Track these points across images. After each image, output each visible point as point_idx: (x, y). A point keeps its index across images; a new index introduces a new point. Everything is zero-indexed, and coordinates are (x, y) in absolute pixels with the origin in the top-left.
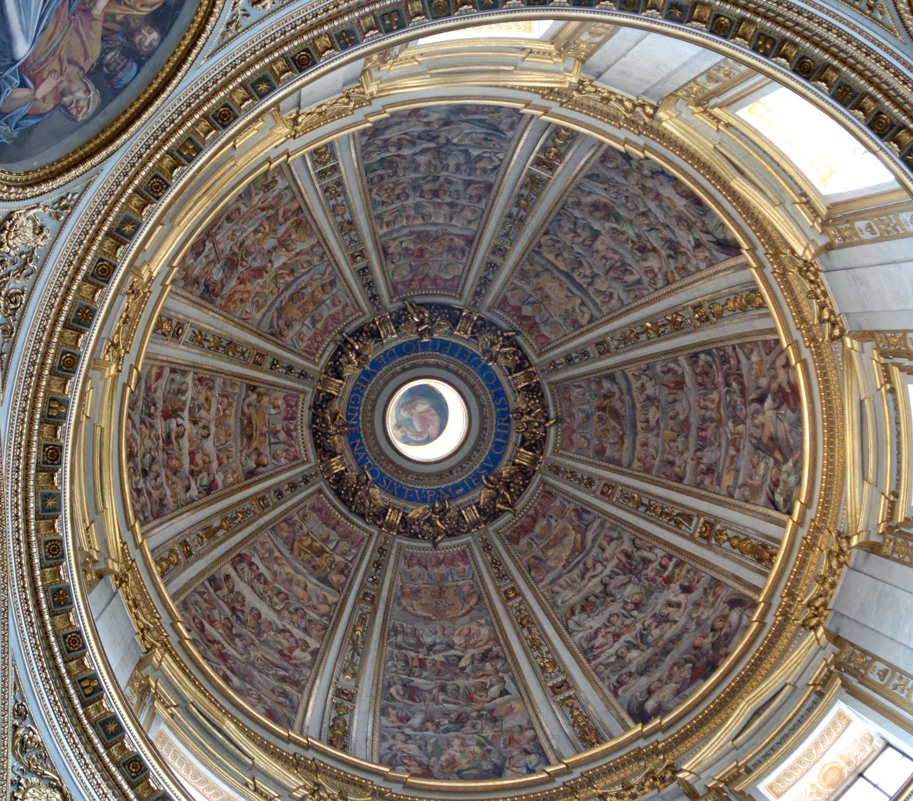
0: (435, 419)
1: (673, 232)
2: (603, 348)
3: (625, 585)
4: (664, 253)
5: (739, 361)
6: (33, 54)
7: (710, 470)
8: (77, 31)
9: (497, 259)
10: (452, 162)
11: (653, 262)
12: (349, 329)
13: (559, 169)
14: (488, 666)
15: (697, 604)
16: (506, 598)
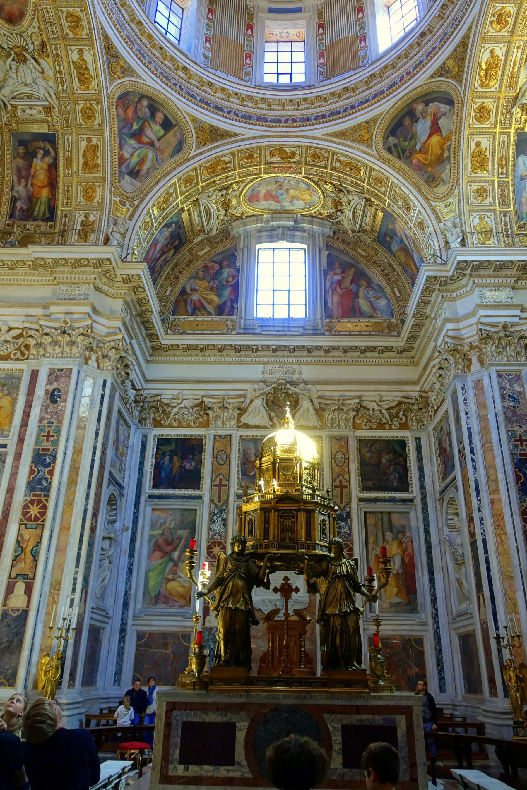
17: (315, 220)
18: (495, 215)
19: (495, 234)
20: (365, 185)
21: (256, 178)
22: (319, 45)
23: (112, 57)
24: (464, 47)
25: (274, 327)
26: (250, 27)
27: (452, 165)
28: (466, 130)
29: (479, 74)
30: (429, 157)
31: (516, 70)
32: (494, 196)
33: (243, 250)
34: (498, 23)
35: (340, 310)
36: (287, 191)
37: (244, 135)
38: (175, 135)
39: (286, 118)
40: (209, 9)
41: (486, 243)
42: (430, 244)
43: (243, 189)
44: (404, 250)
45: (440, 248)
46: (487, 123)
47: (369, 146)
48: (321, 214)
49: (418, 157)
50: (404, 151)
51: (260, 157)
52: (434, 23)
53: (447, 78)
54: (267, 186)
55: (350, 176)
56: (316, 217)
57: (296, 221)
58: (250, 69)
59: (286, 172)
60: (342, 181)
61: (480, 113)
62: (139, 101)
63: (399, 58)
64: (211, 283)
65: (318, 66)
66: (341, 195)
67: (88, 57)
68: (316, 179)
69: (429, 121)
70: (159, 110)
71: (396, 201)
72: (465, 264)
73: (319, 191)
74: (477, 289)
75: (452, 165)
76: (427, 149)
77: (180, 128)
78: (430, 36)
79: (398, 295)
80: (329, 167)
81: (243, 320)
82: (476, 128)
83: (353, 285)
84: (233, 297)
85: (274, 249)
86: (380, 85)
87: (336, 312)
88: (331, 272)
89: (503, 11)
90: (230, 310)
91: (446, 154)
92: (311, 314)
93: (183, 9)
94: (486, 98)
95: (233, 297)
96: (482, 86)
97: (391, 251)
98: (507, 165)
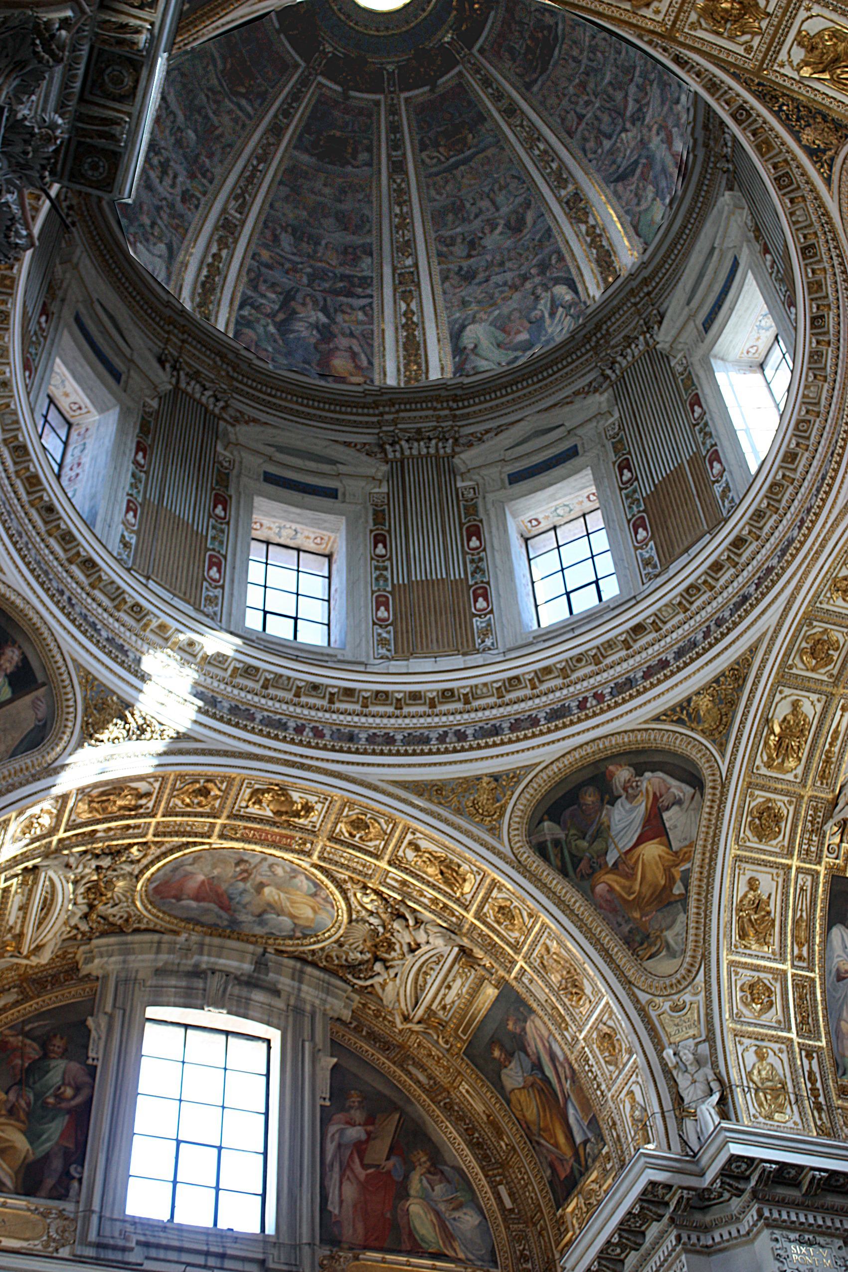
3: (195, 131)
4: (465, 264)
5: (359, 297)
7: (276, 238)
10: (606, 118)
11: (460, 250)
15: (172, 206)
17: (309, 969)
18: (790, 1051)
19: (792, 1097)
20: (470, 916)
21: (195, 844)
22: (377, 579)
24: (736, 680)
25: (180, 1250)
26: (222, 500)
27: (692, 917)
28: (729, 850)
29: (766, 743)
30: (637, 888)
31: (836, 749)
32: (785, 1007)
33: (111, 1017)
34: (813, 655)
35: (360, 1226)
36: (260, 887)
37: (200, 741)
38: (34, 705)
39: (300, 722)
40: (138, 443)
41: (777, 1116)
42: (631, 1092)
43: (152, 863)
44: (541, 1091)
45: (663, 1113)
46: (774, 842)
47: (493, 831)
48: (328, 957)
49: (607, 882)
50: (576, 860)
53: (692, 730)
54: (214, 866)
55: (434, 887)
56: (314, 965)
57: (261, 963)
58: (218, 592)
59: (274, 845)
60: (409, 894)
61: (760, 819)
63: (579, 660)
64: (12, 1096)
65: (374, 624)
66: (396, 925)
68: (343, 875)
69: (641, 809)
70: (14, 642)
71: (543, 969)
72: (744, 1166)
73: (342, 904)
74: (766, 1233)
75: (692, 917)
76: (634, 868)
77: (50, 693)
79: (508, 1204)
80: (387, 858)
81: (95, 1219)
82: (751, 849)
83: (394, 1160)
84: (71, 1146)
85: (187, 1026)
86: (530, 703)
87: (352, 1231)
88: (339, 1116)
89: (825, 637)
90: (59, 1182)
91: (678, 889)
92: (284, 1228)
93: (70, 425)
94: (775, 791)
95: (71, 1146)
96: (769, 766)
97: (498, 1085)
98: (810, 940)
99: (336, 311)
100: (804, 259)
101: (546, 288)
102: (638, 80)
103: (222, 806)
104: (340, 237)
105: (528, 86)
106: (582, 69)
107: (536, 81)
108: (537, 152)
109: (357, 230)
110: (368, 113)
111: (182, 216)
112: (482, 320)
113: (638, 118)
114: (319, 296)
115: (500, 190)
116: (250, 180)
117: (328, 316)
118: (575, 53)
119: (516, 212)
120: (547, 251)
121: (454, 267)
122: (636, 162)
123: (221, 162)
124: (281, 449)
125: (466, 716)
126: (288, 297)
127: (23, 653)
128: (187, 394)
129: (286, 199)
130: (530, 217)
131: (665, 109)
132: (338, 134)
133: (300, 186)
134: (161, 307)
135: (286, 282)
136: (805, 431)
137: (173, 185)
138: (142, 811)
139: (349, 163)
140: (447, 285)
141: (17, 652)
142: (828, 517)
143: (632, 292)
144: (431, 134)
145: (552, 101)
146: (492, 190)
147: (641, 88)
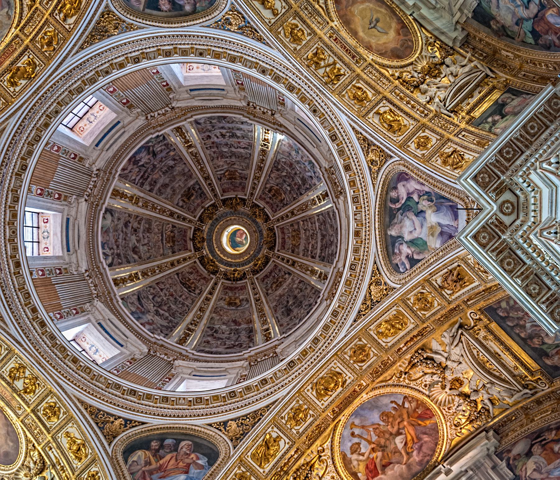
0: (238, 233)
1: (122, 228)
2: (172, 214)
3: (225, 152)
4: (130, 225)
6: (181, 473)
8: (166, 467)
9: (176, 264)
10: (159, 300)
11: (136, 225)
12: (230, 282)
13: (134, 272)
14: (279, 167)
15: (210, 131)
16: (259, 178)
21: (19, 22)
22: (65, 150)
23: (246, 26)
37: (73, 56)
51: (40, 50)
52: (20, 279)
62: (195, 5)
63: (13, 232)
67: (267, 14)
78: (13, 271)
99: (140, 169)
100: (163, 397)
101: (112, 254)
102: (170, 318)
103: (36, 47)
104: (161, 181)
105: (178, 274)
106: (178, 297)
107: (178, 278)
108: (156, 268)
109: (159, 190)
110: (193, 212)
111: (205, 132)
112: (111, 224)
113: (157, 313)
114: (148, 166)
115: (148, 249)
116: (198, 161)
117: (140, 166)
118: (184, 297)
119: (139, 252)
120: (123, 259)
121: (131, 220)
122: (143, 306)
123: (210, 155)
124: (124, 132)
125: (11, 171)
126: (154, 154)
127: (163, 11)
128: (163, 108)
129: (183, 170)
130: (136, 257)
131: (159, 325)
132: (192, 198)
133: (184, 176)
134: (193, 113)
135: (159, 156)
136: (85, 371)
137: (215, 135)
138: (57, 12)
139: (182, 197)
140: (127, 215)
141: (165, 9)
142: (54, 373)
143: (109, 293)
144: (176, 232)
145: (170, 281)
146: (149, 246)
147: (166, 318)
